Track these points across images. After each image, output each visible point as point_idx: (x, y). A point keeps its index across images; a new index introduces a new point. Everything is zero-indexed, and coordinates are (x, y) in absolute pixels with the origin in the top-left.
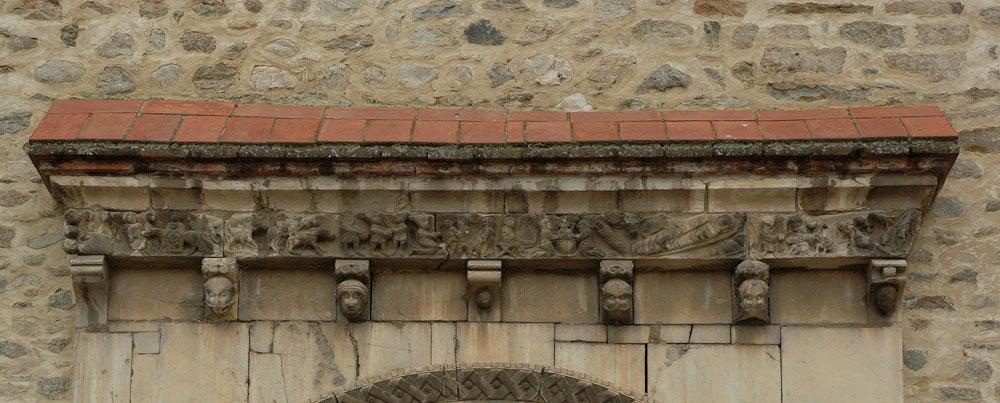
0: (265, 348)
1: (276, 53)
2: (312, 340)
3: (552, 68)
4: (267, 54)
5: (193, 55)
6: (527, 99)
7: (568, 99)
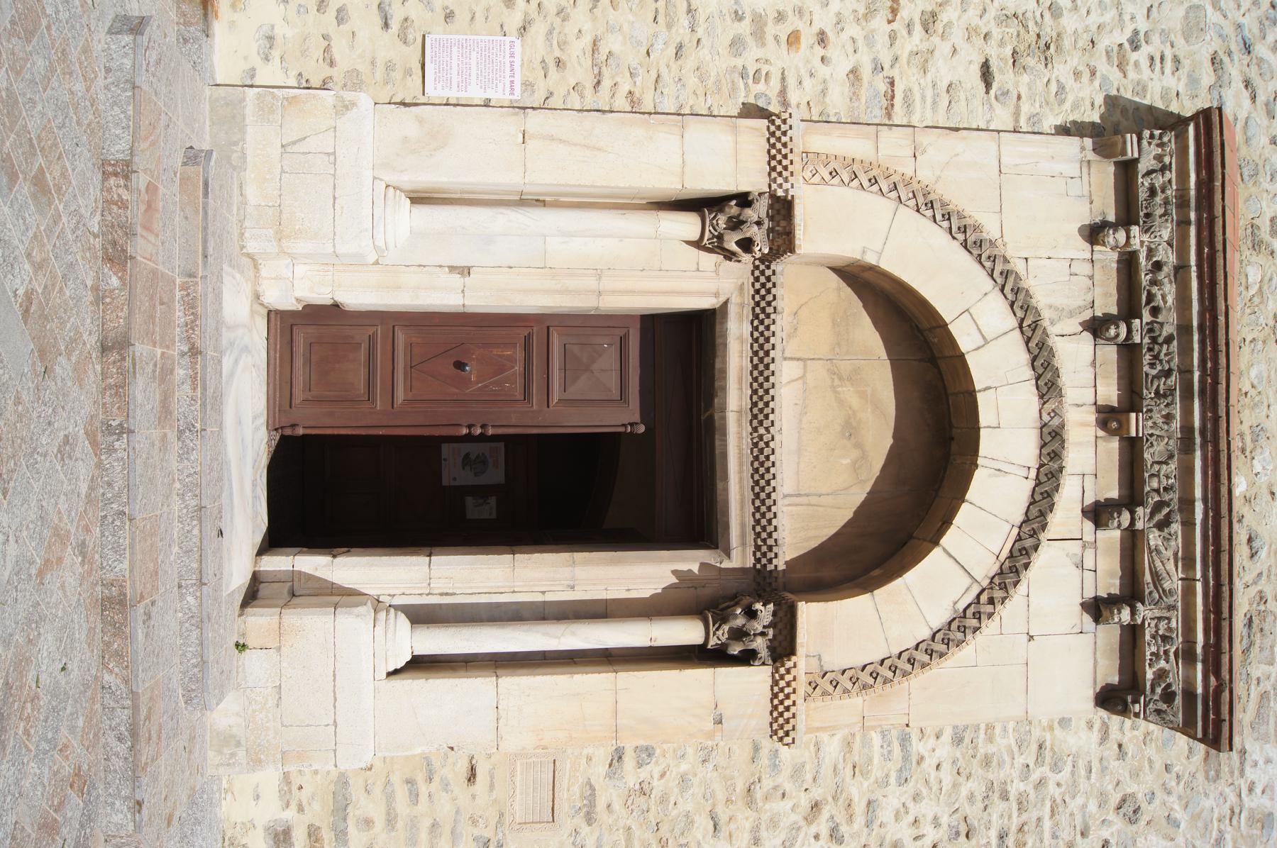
0: (1074, 270)
1: (1271, 280)
2: (1082, 303)
3: (1264, 468)
4: (1268, 275)
5: (1268, 223)
6: (1243, 451)
7: (1243, 479)
